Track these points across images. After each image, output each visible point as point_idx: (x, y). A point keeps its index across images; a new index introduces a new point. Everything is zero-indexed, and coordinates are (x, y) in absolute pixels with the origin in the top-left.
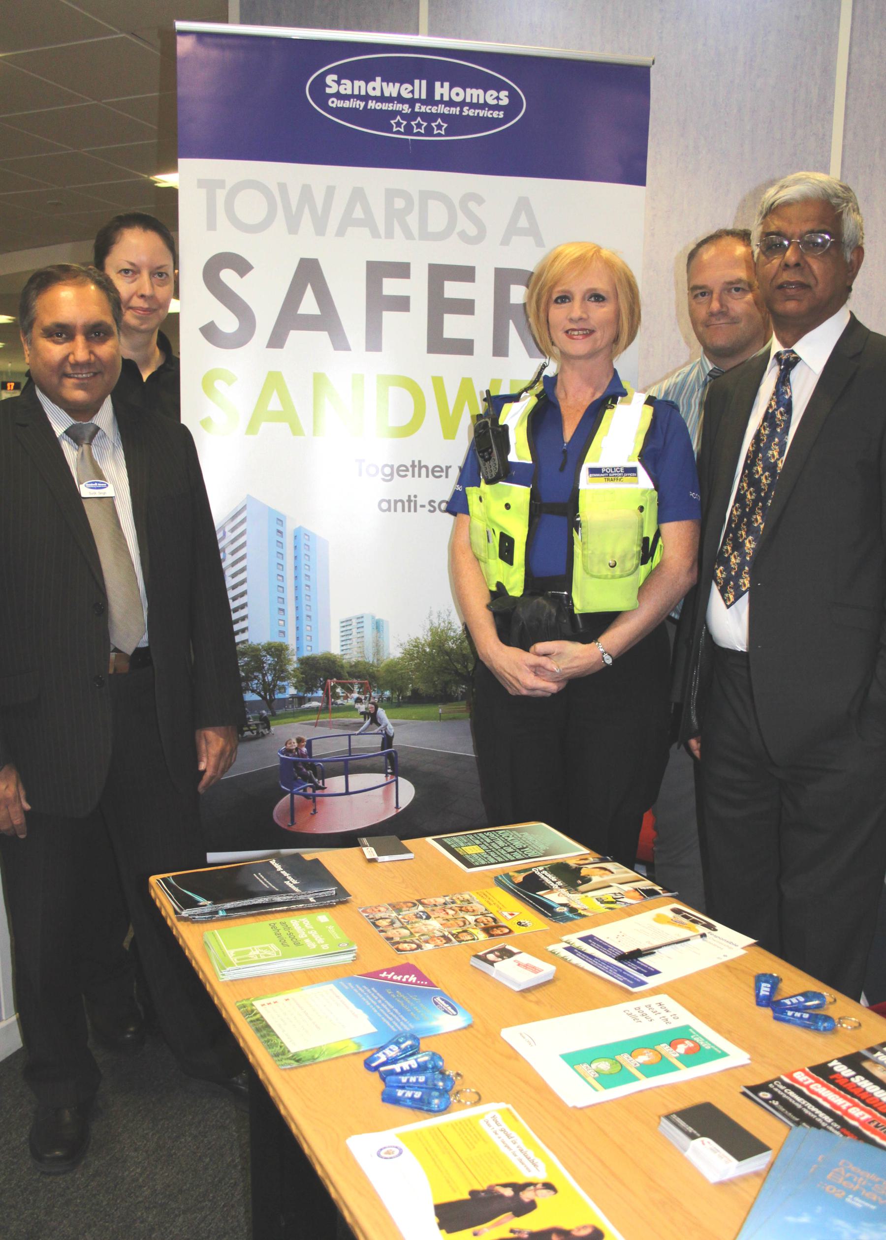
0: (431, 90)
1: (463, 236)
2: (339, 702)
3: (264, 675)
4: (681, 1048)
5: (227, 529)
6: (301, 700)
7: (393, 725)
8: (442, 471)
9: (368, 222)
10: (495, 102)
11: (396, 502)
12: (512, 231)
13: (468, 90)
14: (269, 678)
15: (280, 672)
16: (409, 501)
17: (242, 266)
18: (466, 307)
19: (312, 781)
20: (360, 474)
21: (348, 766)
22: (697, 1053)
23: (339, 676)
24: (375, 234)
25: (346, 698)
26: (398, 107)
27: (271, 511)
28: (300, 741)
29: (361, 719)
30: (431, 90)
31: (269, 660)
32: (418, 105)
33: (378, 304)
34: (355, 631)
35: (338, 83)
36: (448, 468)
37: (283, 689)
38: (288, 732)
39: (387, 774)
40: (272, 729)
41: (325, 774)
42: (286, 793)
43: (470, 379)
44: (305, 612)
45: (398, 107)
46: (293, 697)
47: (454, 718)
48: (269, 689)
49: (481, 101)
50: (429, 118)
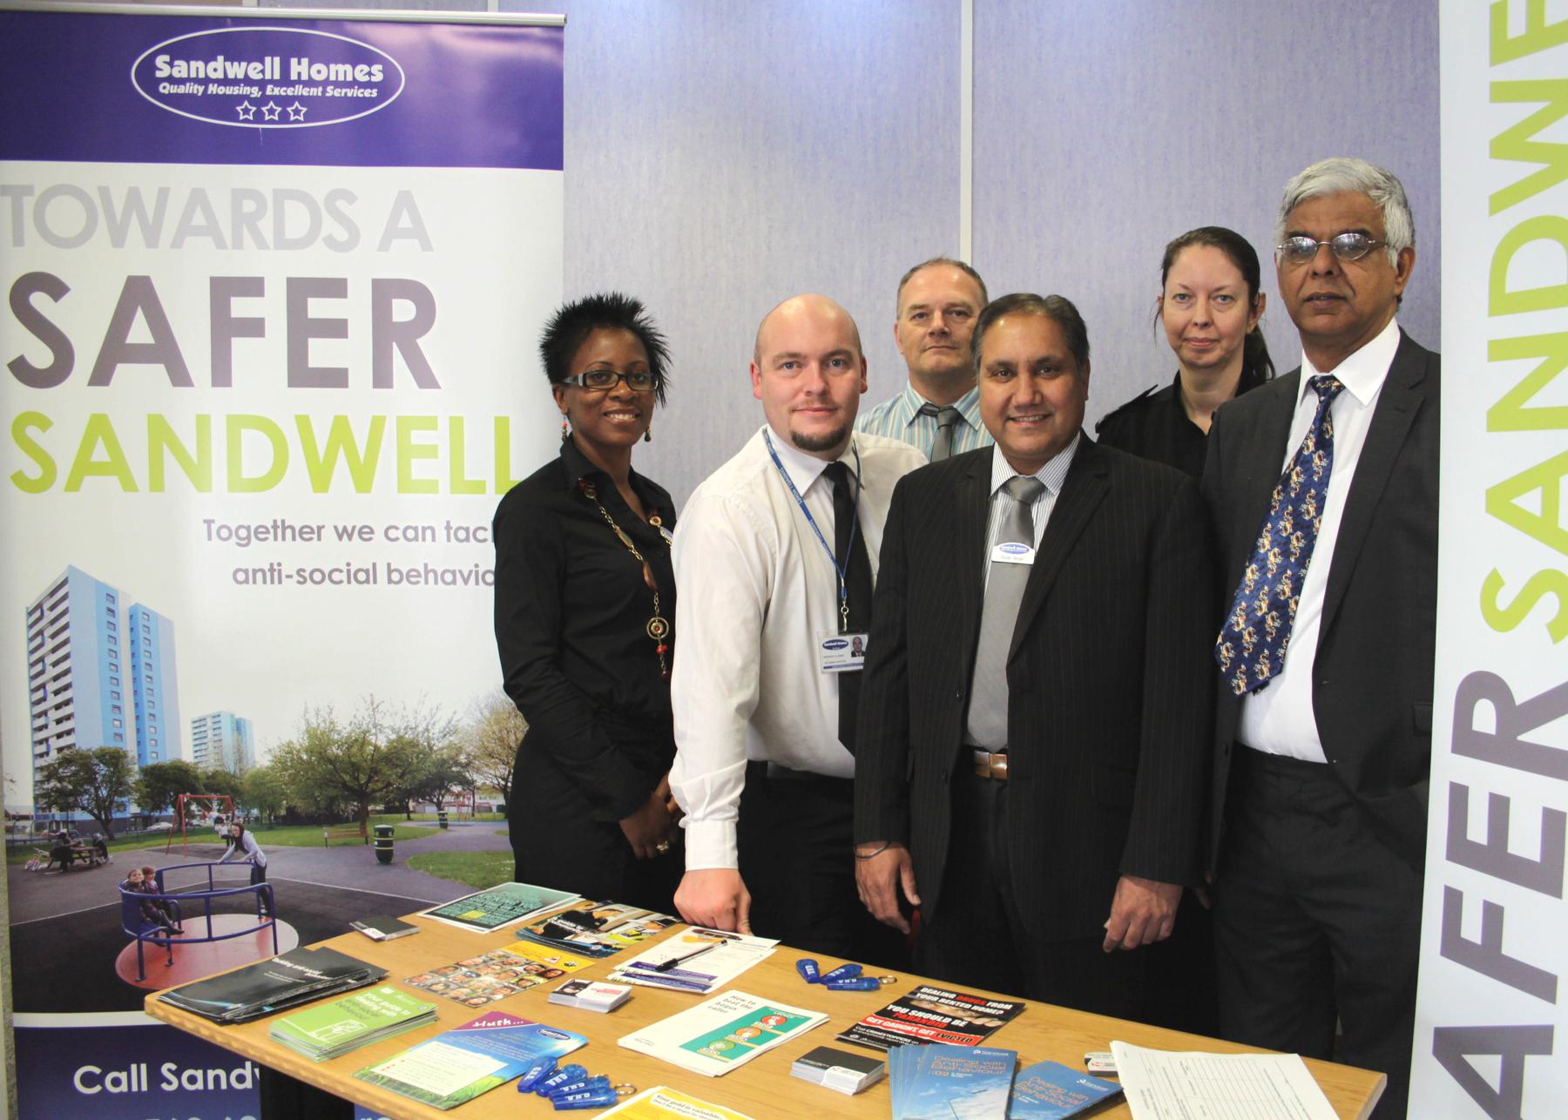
0: (285, 69)
1: (331, 242)
2: (195, 822)
3: (97, 789)
4: (772, 1022)
5: (46, 606)
6: (147, 820)
7: (266, 852)
8: (312, 532)
9: (212, 229)
10: (366, 79)
11: (255, 572)
12: (393, 231)
13: (333, 67)
14: (104, 792)
15: (117, 784)
16: (272, 570)
17: (56, 288)
18: (337, 329)
19: (165, 923)
20: (210, 538)
21: (210, 903)
22: (785, 1023)
23: (194, 790)
24: (221, 244)
25: (204, 817)
26: (245, 90)
27: (103, 586)
28: (147, 872)
29: (223, 844)
30: (285, 69)
31: (103, 770)
32: (269, 87)
33: (225, 329)
34: (210, 733)
35: (171, 64)
36: (320, 528)
37: (123, 806)
38: (131, 860)
39: (261, 916)
40: (110, 856)
41: (182, 914)
42: (131, 939)
43: (345, 418)
44: (147, 711)
45: (245, 90)
46: (135, 816)
47: (345, 844)
48: (104, 806)
49: (350, 78)
50: (284, 101)
